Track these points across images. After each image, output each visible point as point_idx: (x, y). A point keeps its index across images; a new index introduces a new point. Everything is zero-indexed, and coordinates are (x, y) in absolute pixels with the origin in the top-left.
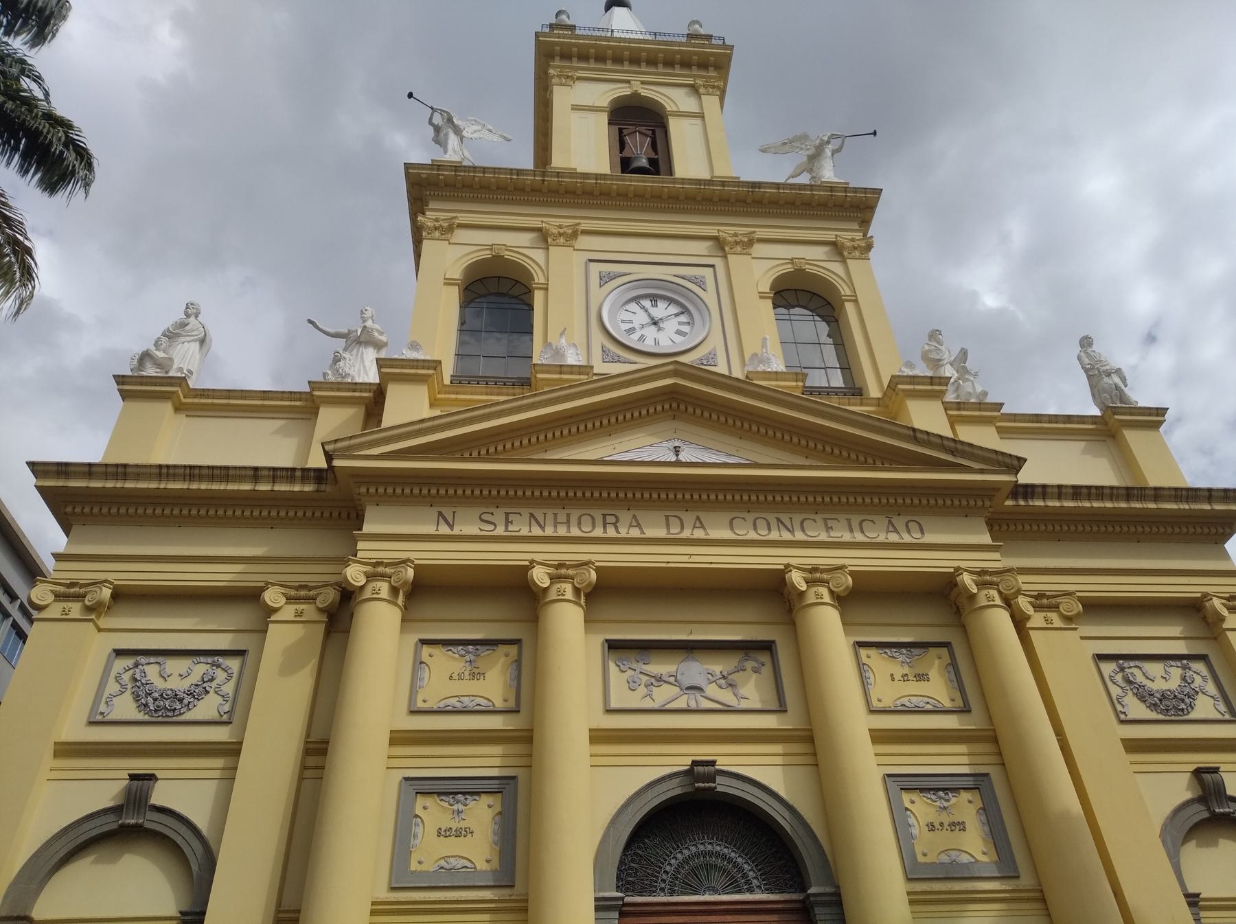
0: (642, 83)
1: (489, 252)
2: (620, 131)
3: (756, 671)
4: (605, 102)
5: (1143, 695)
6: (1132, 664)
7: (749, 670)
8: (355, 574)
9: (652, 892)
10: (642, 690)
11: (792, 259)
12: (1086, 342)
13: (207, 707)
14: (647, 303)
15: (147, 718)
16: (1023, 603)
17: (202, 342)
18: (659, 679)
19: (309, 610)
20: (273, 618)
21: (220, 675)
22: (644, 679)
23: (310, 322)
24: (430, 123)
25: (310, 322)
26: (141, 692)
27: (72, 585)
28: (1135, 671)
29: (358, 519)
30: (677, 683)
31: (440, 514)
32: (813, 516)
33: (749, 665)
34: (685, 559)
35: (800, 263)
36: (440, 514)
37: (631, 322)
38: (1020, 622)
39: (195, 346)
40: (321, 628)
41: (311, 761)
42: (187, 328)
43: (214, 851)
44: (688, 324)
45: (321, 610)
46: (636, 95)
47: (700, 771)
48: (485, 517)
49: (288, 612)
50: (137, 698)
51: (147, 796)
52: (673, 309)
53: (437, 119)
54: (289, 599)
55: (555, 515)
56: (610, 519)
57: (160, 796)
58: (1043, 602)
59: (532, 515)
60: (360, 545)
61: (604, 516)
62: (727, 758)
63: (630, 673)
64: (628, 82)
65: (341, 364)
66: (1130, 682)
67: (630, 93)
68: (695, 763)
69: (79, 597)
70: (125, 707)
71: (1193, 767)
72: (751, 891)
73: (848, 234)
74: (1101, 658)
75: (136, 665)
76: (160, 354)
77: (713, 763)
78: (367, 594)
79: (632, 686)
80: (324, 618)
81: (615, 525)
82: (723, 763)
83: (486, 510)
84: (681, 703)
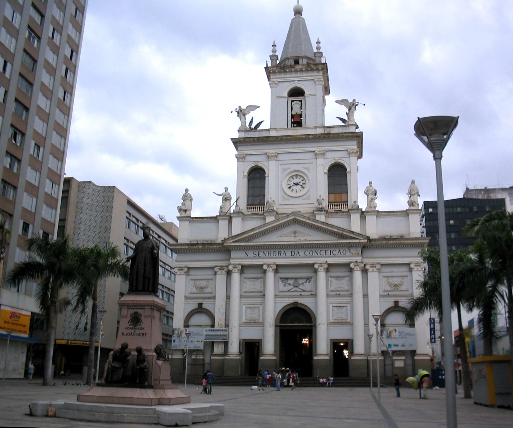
0: (298, 81)
1: (254, 164)
2: (292, 101)
3: (309, 282)
4: (286, 94)
5: (391, 285)
6: (391, 278)
7: (308, 282)
8: (231, 268)
9: (286, 323)
10: (286, 287)
11: (335, 158)
12: (413, 182)
13: (208, 290)
14: (295, 177)
15: (198, 292)
16: (367, 267)
17: (191, 200)
18: (290, 284)
19: (224, 272)
20: (217, 273)
21: (210, 284)
22: (287, 284)
23: (213, 192)
24: (236, 111)
25: (213, 192)
26: (197, 287)
27: (180, 267)
28: (391, 280)
29: (230, 260)
30: (293, 285)
31: (245, 253)
32: (322, 250)
33: (308, 281)
34: (295, 262)
35: (337, 160)
36: (245, 253)
37: (290, 184)
38: (365, 271)
39: (189, 202)
40: (226, 275)
41: (228, 300)
42: (187, 197)
43: (214, 315)
44: (304, 184)
45: (226, 272)
46: (296, 87)
47: (296, 303)
48: (254, 253)
49: (220, 272)
50: (196, 289)
51: (202, 306)
52: (302, 179)
53: (237, 110)
54: (219, 269)
55: (268, 252)
56: (280, 253)
57: (204, 306)
58: (373, 265)
59: (263, 252)
60: (231, 260)
61: (278, 252)
62: (300, 300)
63: (284, 283)
64: (294, 81)
65: (222, 209)
66: (388, 282)
67: (294, 86)
68: (294, 302)
69: (182, 270)
70: (194, 290)
71: (394, 301)
72: (303, 323)
73: (352, 146)
74: (384, 277)
75: (195, 282)
76: (184, 208)
77: (297, 302)
78: (233, 271)
79: (285, 286)
80: (226, 273)
81: (280, 254)
82: (299, 302)
83: (254, 251)
84: (294, 290)
